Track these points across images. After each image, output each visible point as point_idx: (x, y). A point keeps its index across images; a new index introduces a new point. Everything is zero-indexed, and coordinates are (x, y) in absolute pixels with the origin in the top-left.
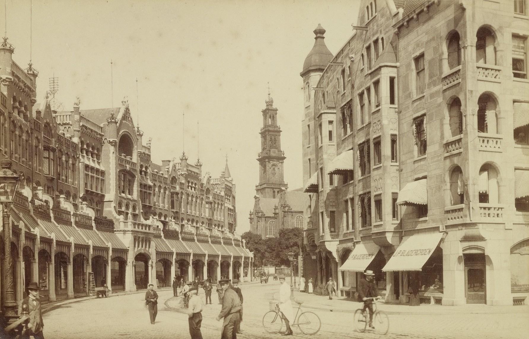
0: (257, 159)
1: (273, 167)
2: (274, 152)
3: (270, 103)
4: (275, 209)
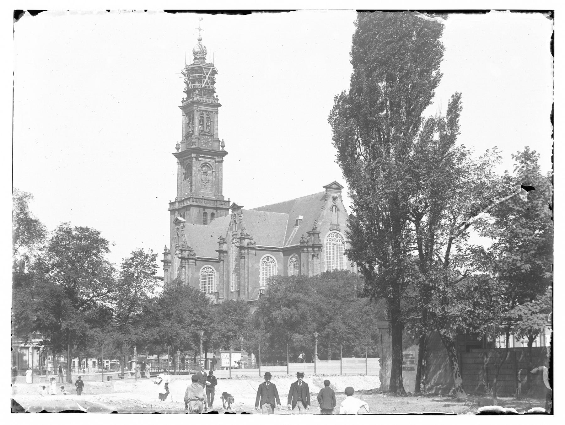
1: (204, 169)
2: (207, 143)
3: (200, 55)
4: (220, 243)
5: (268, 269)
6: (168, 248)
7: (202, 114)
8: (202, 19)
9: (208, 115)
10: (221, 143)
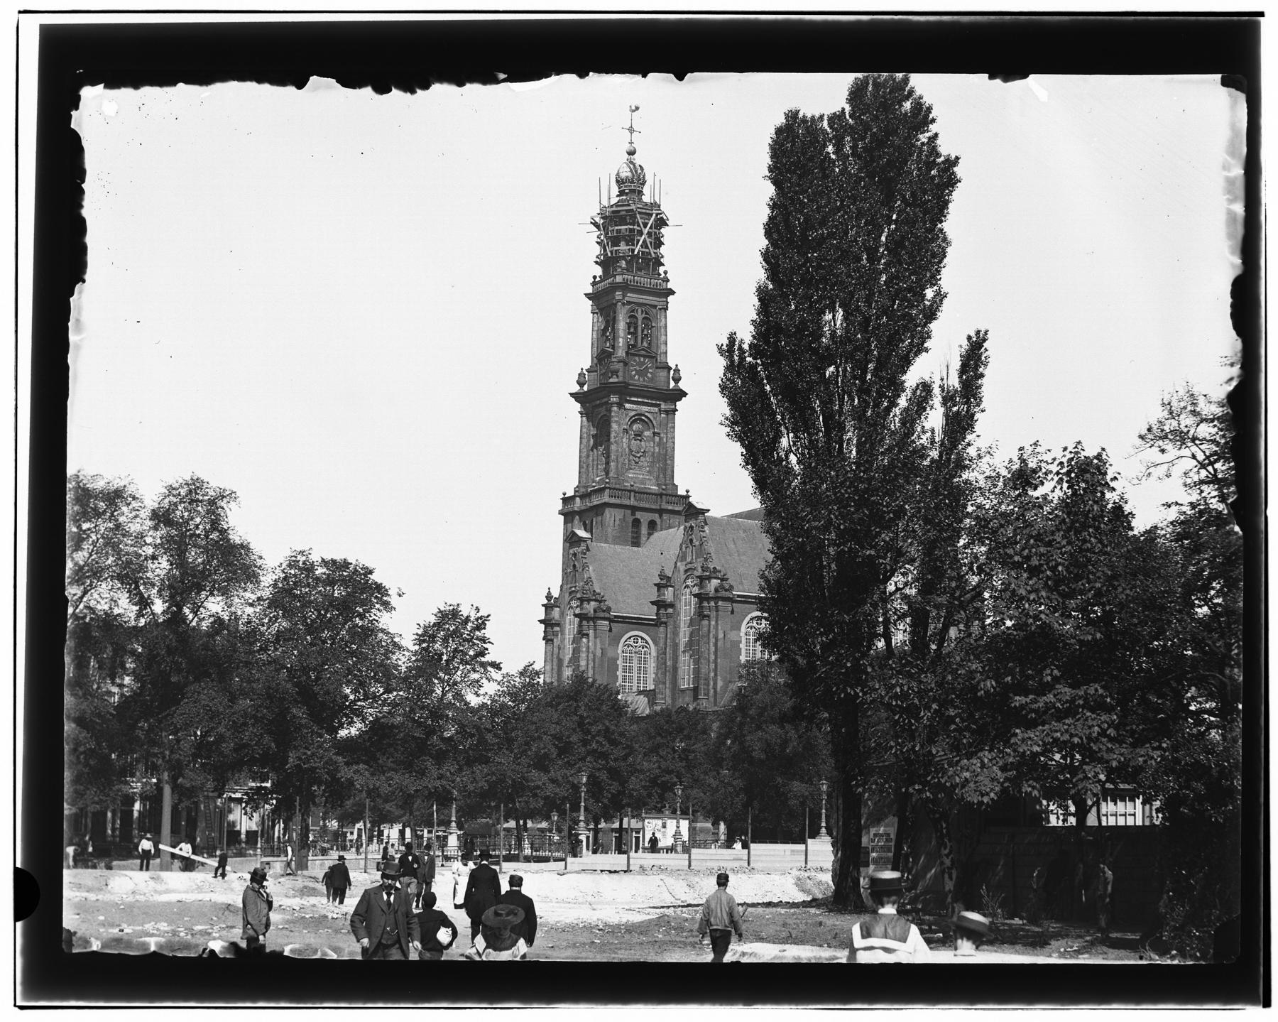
0: (571, 394)
1: (635, 427)
2: (642, 373)
3: (631, 184)
4: (659, 587)
5: (635, 661)
6: (556, 593)
7: (633, 311)
8: (637, 108)
9: (646, 313)
10: (672, 372)
